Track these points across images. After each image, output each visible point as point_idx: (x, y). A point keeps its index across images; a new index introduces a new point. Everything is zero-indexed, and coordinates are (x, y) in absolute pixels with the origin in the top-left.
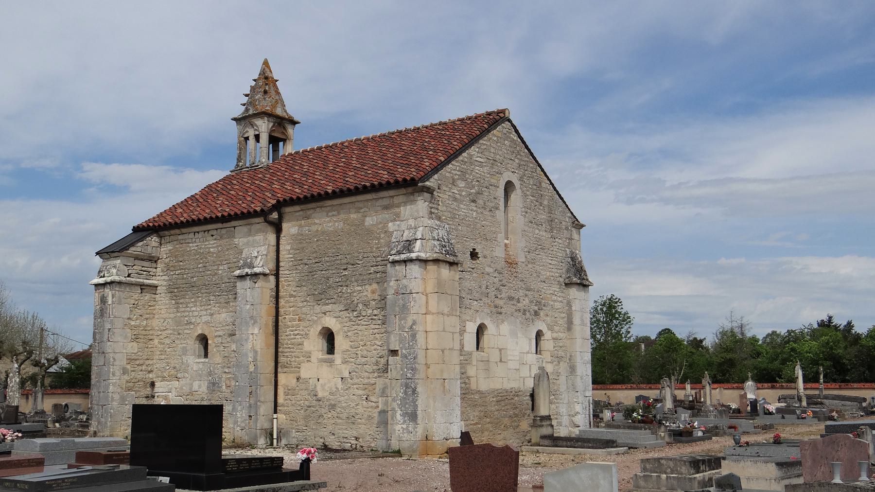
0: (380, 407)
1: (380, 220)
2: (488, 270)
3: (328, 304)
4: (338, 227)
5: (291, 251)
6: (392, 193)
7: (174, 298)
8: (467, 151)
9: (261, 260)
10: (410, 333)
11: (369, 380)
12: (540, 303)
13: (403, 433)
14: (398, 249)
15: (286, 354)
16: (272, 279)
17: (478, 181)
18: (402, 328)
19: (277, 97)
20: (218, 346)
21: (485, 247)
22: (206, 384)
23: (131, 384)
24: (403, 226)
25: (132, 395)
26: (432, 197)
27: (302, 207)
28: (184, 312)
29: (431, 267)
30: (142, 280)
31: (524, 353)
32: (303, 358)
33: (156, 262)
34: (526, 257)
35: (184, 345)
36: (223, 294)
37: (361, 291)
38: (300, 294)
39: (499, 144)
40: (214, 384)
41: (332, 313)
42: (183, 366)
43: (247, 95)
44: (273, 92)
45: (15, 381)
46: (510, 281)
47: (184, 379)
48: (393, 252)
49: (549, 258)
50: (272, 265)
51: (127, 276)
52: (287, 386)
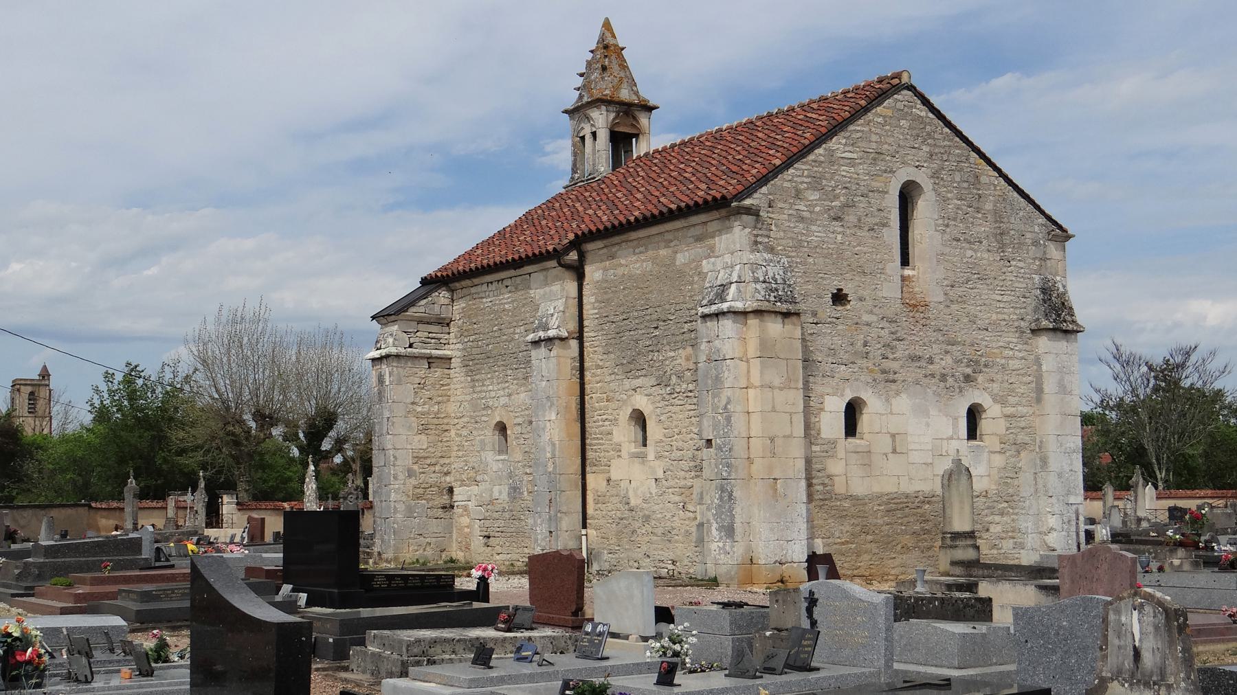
0: (698, 519)
1: (692, 257)
2: (866, 318)
3: (638, 377)
4: (646, 268)
5: (596, 305)
6: (702, 217)
7: (470, 374)
8: (824, 146)
9: (557, 319)
10: (724, 415)
11: (686, 482)
12: (977, 362)
13: (720, 554)
14: (711, 298)
15: (595, 447)
16: (574, 344)
17: (846, 188)
18: (715, 409)
19: (622, 74)
20: (518, 438)
21: (861, 285)
22: (507, 489)
23: (420, 491)
24: (719, 263)
25: (423, 505)
26: (757, 221)
27: (604, 242)
28: (480, 392)
29: (753, 322)
30: (428, 351)
32: (613, 453)
33: (448, 325)
34: (946, 294)
35: (482, 437)
36: (521, 366)
37: (675, 358)
38: (607, 364)
39: (888, 127)
41: (643, 389)
42: (482, 466)
43: (581, 75)
44: (615, 67)
45: (312, 488)
47: (483, 483)
48: (704, 302)
49: (996, 292)
50: (573, 325)
51: (407, 346)
52: (597, 491)
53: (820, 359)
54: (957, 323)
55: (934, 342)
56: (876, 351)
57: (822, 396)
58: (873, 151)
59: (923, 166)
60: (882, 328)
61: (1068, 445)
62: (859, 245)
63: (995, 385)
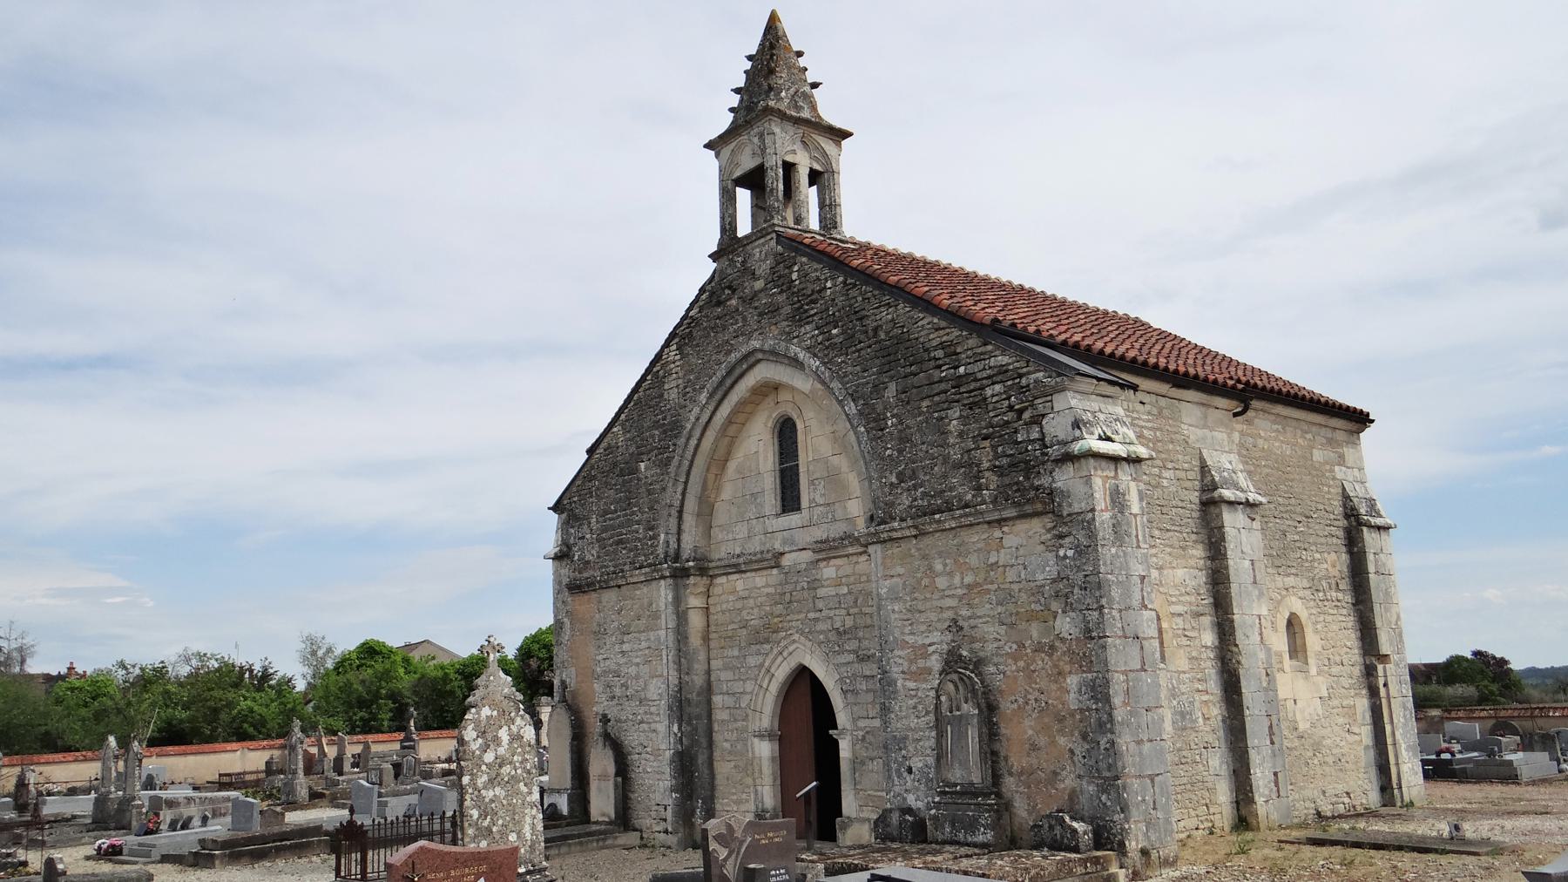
3: (1288, 575)
40: (1183, 715)
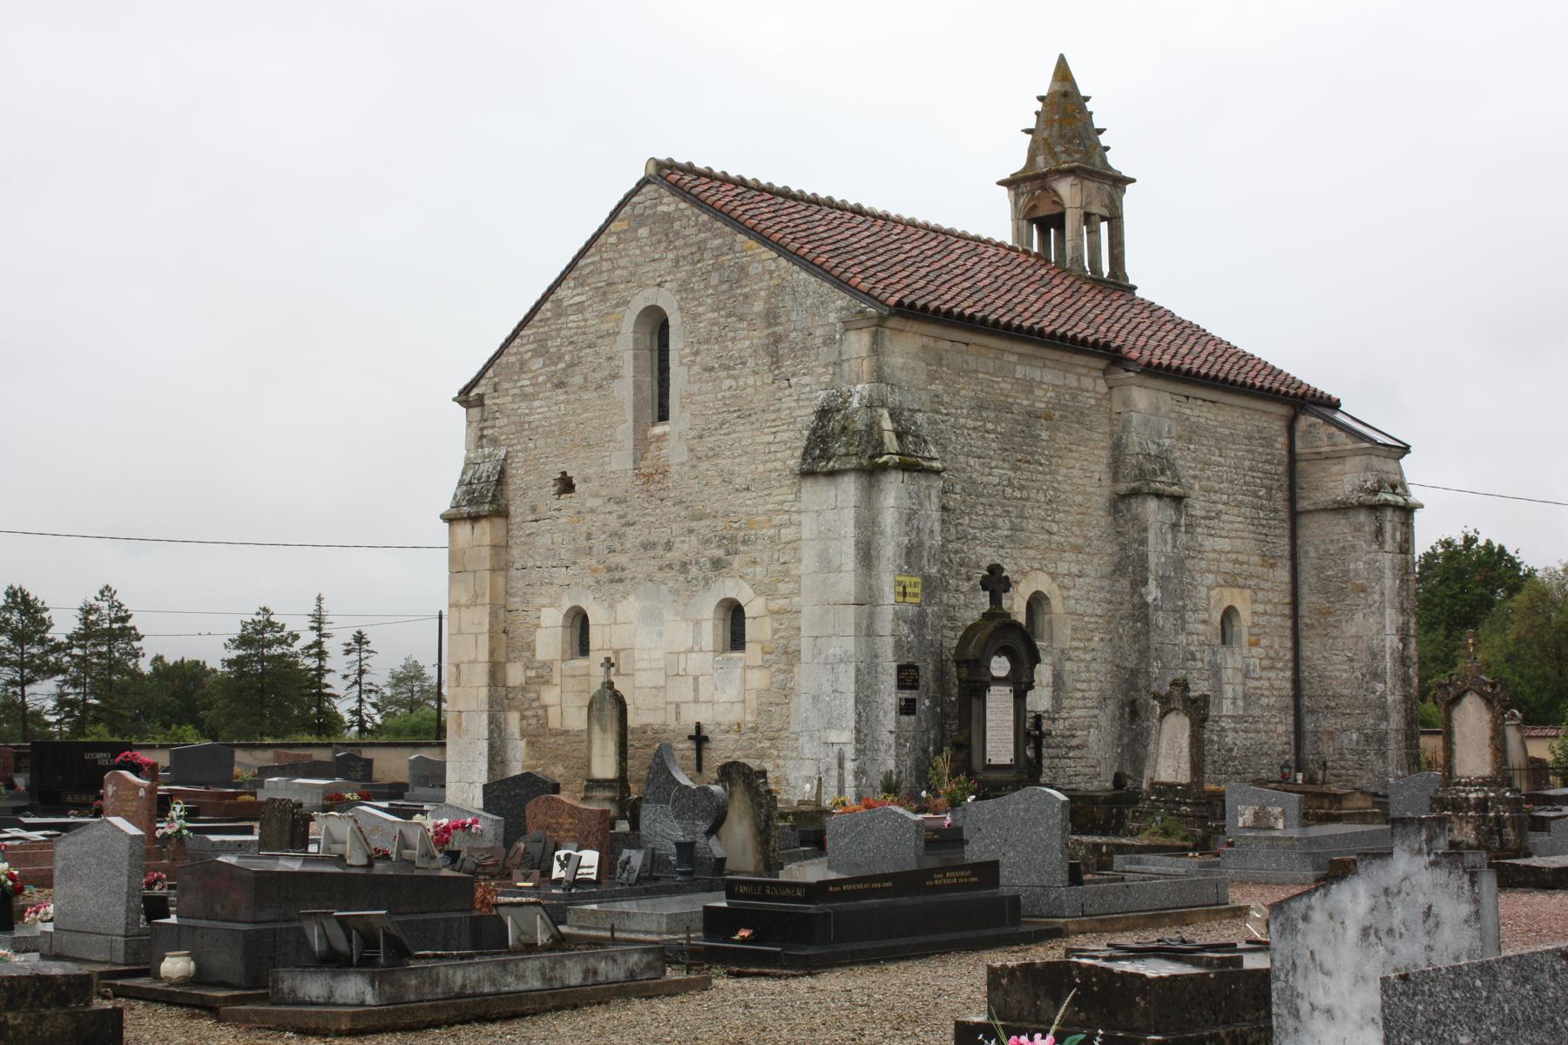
17: (572, 343)
31: (678, 653)
34: (691, 450)
46: (646, 511)
49: (766, 430)
53: (539, 564)
54: (706, 488)
55: (675, 521)
56: (600, 542)
57: (539, 610)
58: (603, 284)
59: (666, 281)
60: (610, 513)
61: (831, 651)
62: (586, 410)
63: (758, 569)
